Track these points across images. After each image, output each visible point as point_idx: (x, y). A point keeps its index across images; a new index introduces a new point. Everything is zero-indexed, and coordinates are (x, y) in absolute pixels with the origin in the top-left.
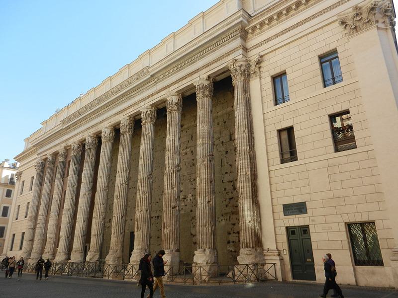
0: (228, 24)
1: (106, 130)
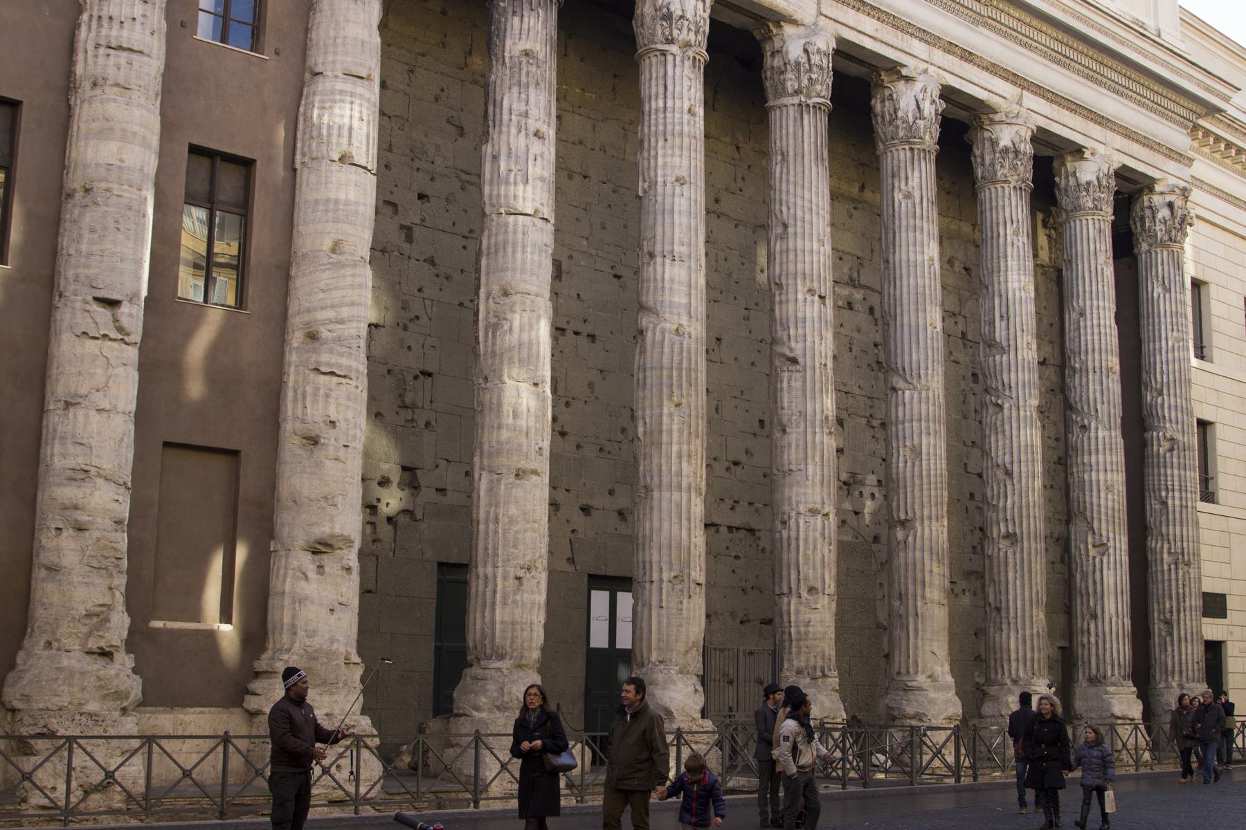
0: (1208, 89)
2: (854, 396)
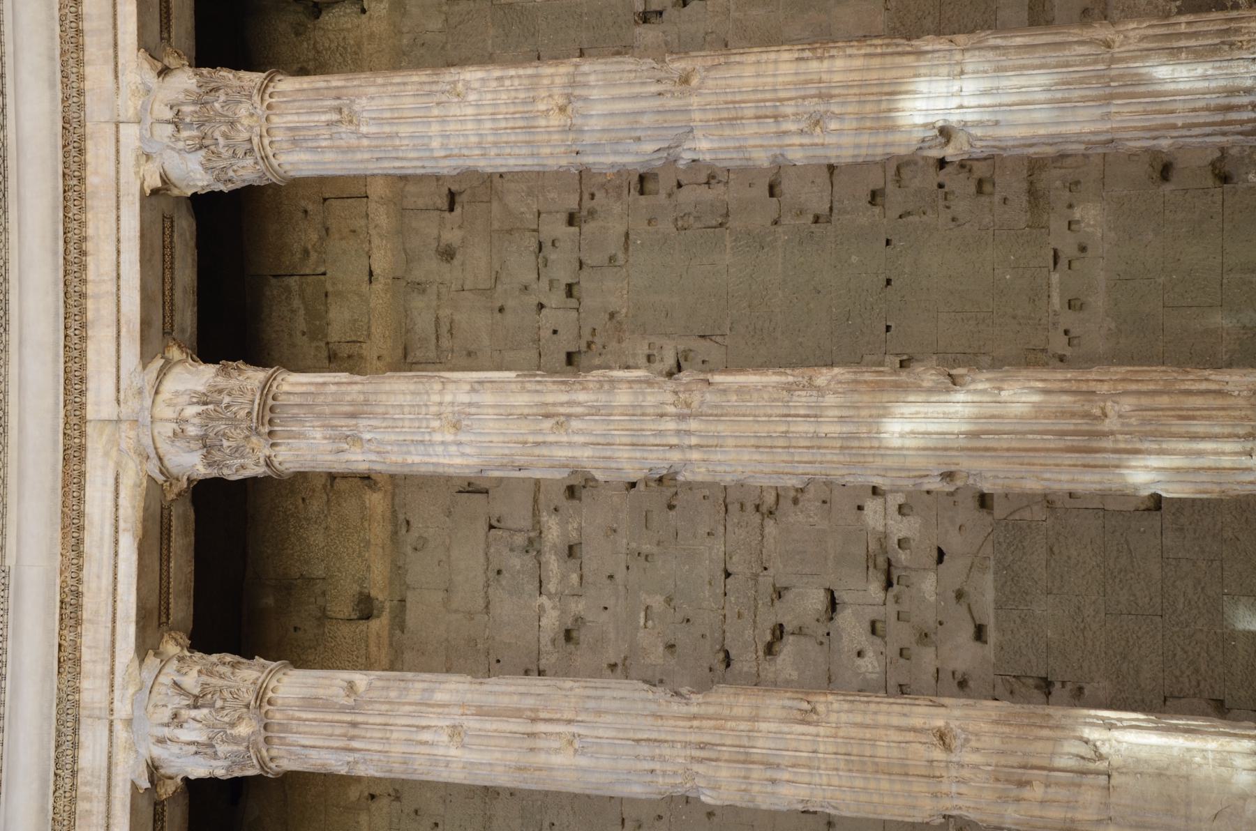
2: (727, 556)
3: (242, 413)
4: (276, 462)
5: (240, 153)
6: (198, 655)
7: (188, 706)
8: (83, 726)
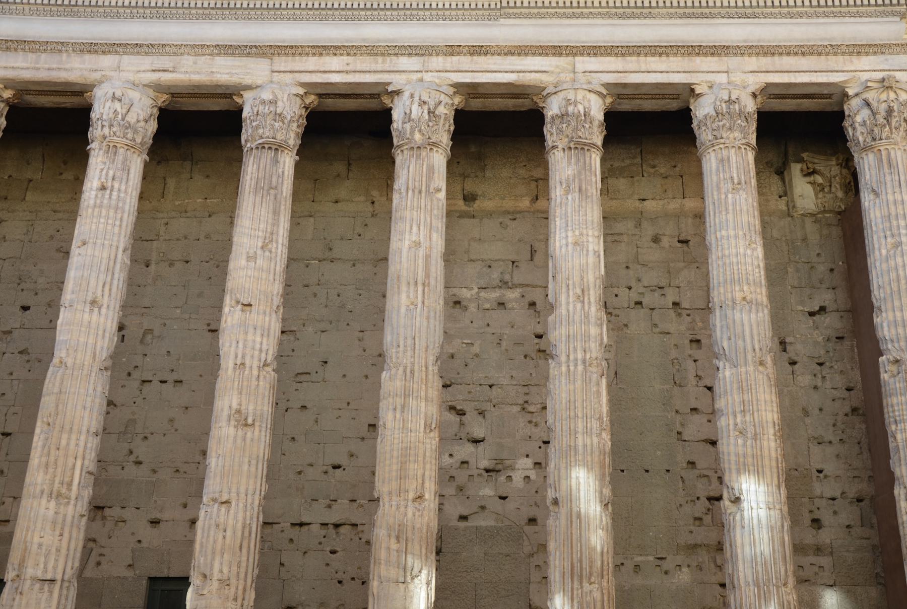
1: (135, 95)
2: (501, 386)
3: (580, 134)
4: (555, 151)
5: (714, 133)
6: (453, 113)
7: (429, 109)
8: (419, 58)
